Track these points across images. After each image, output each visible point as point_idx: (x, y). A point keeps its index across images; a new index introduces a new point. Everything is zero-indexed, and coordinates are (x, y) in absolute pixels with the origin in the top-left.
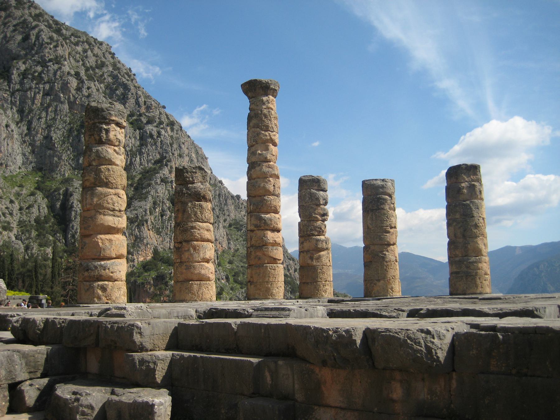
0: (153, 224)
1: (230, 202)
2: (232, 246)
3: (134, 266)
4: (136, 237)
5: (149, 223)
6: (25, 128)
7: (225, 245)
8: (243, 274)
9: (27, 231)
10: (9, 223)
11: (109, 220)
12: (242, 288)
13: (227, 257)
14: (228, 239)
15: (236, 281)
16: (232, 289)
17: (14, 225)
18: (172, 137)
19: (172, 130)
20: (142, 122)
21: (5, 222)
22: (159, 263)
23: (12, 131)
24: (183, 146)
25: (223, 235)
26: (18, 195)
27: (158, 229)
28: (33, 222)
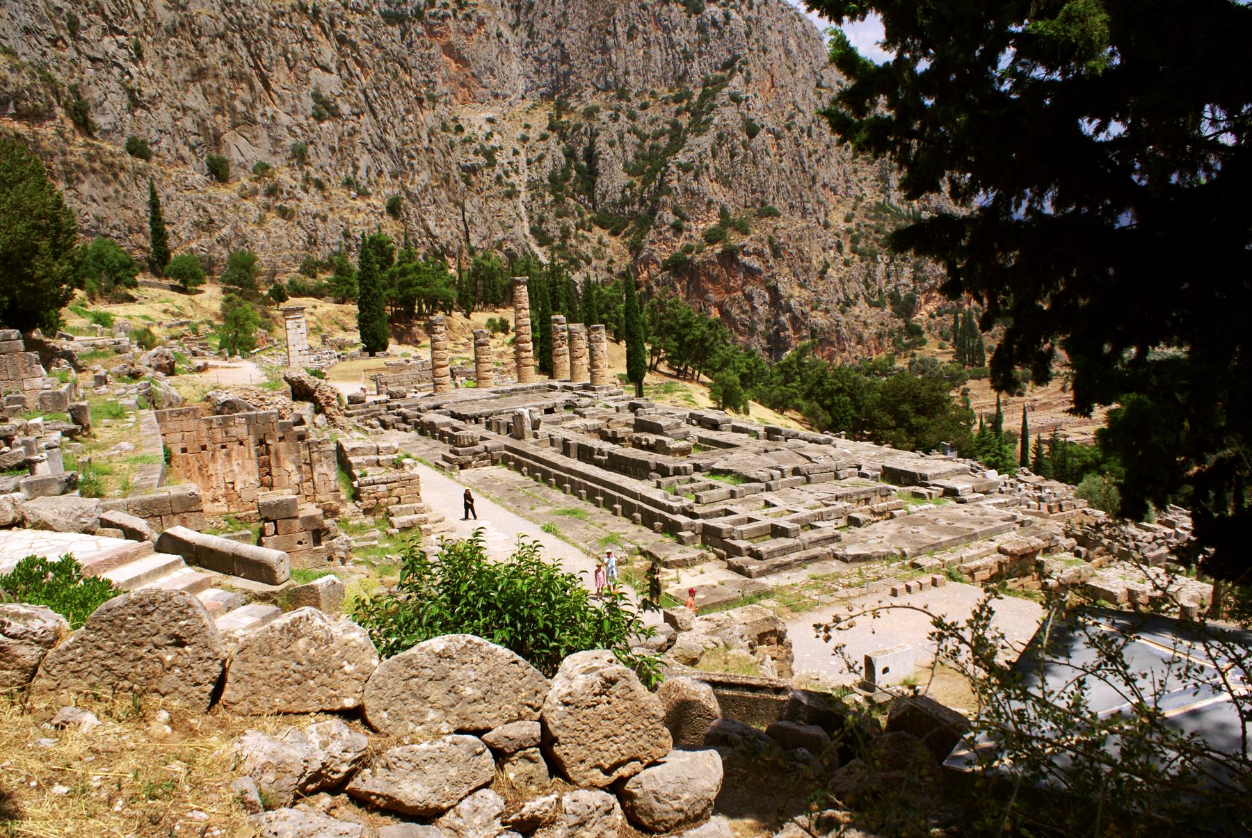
0: (717, 170)
2: (855, 191)
3: (691, 237)
4: (693, 194)
5: (712, 170)
6: (524, 35)
8: (867, 237)
9: (540, 195)
10: (513, 185)
11: (441, 363)
14: (847, 181)
15: (854, 251)
16: (846, 263)
18: (749, 19)
19: (750, 8)
21: (508, 185)
22: (729, 231)
23: (507, 42)
24: (768, 33)
26: (524, 139)
28: (546, 182)
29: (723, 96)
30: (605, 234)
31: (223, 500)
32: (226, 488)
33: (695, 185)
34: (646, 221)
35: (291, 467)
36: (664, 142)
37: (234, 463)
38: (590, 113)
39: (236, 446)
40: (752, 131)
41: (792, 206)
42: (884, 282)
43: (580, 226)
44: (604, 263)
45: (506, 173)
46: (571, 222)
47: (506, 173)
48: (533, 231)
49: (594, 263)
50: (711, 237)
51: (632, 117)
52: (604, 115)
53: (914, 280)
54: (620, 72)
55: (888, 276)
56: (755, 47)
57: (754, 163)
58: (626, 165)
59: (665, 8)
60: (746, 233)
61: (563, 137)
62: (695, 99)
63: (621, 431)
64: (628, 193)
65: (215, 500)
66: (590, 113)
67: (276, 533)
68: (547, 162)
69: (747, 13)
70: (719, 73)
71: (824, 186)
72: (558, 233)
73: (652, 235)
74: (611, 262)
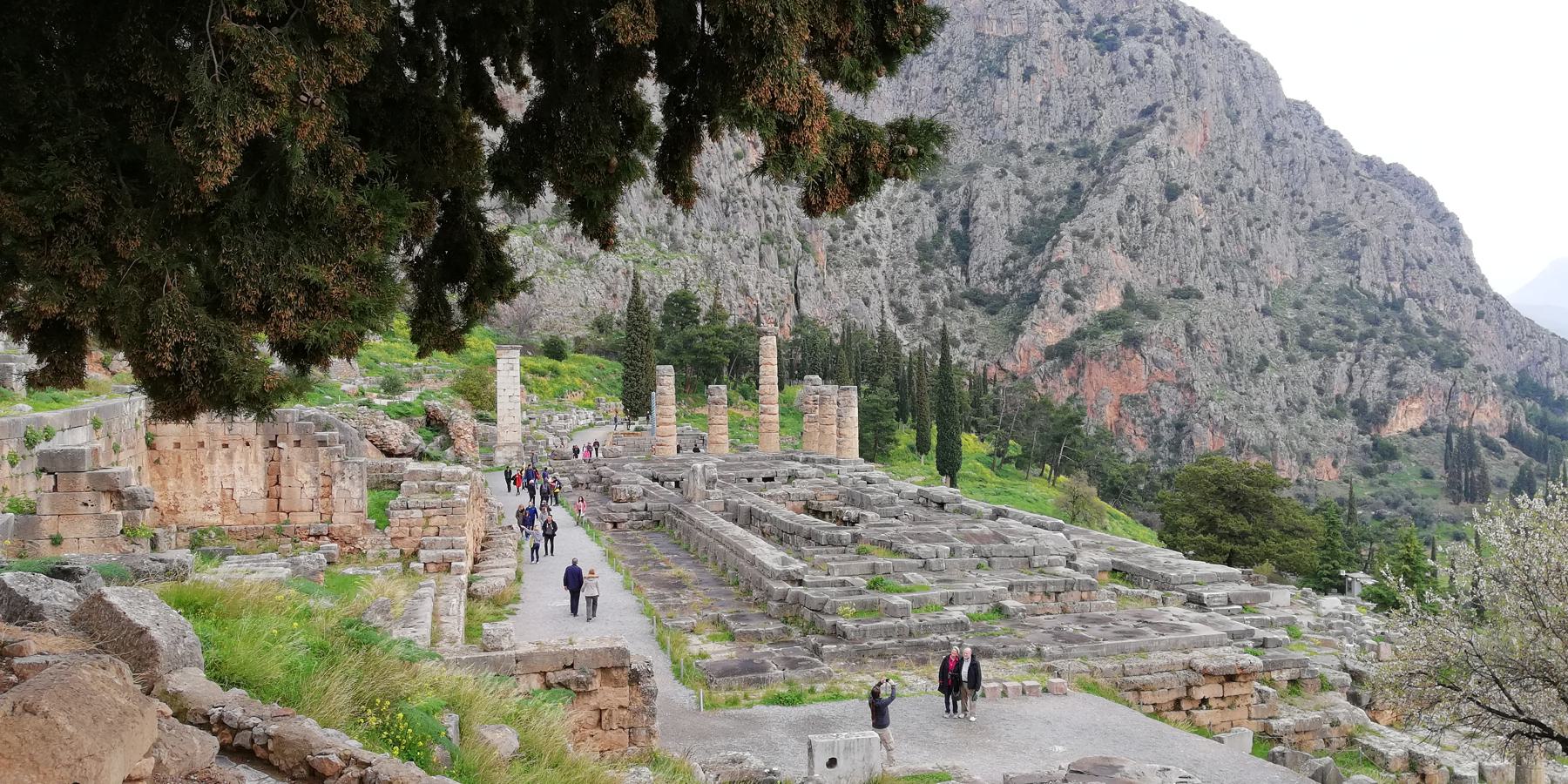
1: (1315, 175)
7: (1290, 271)
10: (873, 253)
12: (1314, 358)
13: (1292, 295)
15: (1304, 345)
16: (1291, 360)
17: (883, 255)
18: (1178, 57)
19: (1181, 42)
20: (1117, 34)
21: (864, 251)
24: (1203, 73)
25: (1285, 250)
27: (1136, 249)
28: (914, 250)
29: (1139, 150)
30: (976, 312)
31: (218, 509)
32: (224, 495)
33: (1094, 257)
34: (1032, 299)
35: (307, 478)
36: (1060, 205)
37: (236, 466)
38: (971, 169)
39: (240, 447)
40: (1172, 193)
41: (1220, 287)
42: (1345, 386)
43: (952, 303)
44: (975, 347)
45: (867, 238)
46: (936, 297)
47: (867, 238)
48: (892, 304)
49: (963, 346)
50: (1109, 321)
51: (1022, 174)
52: (988, 173)
53: (1389, 385)
54: (1012, 120)
55: (1351, 379)
56: (1184, 90)
57: (1173, 231)
58: (1010, 231)
59: (1072, 44)
60: (1156, 317)
61: (938, 196)
62: (1102, 154)
63: (827, 504)
64: (1010, 265)
65: (208, 508)
66: (971, 169)
67: (55, 489)
68: (914, 227)
69: (1175, 49)
70: (1134, 123)
71: (1268, 261)
72: (922, 309)
73: (1036, 314)
74: (984, 346)
